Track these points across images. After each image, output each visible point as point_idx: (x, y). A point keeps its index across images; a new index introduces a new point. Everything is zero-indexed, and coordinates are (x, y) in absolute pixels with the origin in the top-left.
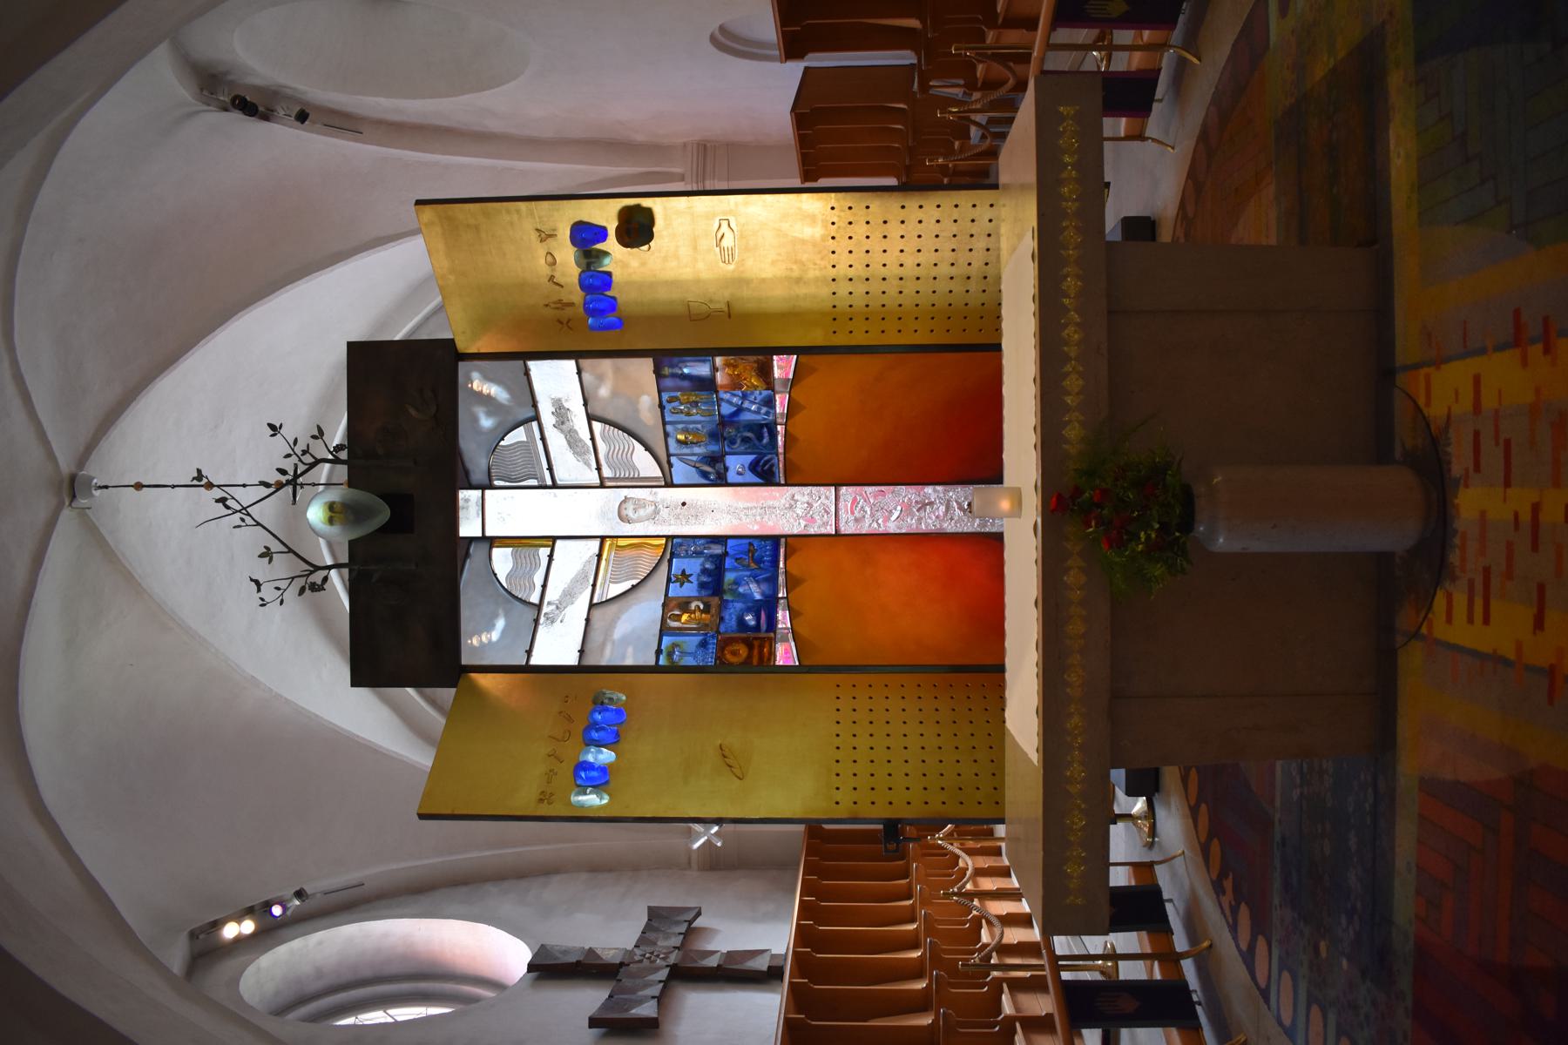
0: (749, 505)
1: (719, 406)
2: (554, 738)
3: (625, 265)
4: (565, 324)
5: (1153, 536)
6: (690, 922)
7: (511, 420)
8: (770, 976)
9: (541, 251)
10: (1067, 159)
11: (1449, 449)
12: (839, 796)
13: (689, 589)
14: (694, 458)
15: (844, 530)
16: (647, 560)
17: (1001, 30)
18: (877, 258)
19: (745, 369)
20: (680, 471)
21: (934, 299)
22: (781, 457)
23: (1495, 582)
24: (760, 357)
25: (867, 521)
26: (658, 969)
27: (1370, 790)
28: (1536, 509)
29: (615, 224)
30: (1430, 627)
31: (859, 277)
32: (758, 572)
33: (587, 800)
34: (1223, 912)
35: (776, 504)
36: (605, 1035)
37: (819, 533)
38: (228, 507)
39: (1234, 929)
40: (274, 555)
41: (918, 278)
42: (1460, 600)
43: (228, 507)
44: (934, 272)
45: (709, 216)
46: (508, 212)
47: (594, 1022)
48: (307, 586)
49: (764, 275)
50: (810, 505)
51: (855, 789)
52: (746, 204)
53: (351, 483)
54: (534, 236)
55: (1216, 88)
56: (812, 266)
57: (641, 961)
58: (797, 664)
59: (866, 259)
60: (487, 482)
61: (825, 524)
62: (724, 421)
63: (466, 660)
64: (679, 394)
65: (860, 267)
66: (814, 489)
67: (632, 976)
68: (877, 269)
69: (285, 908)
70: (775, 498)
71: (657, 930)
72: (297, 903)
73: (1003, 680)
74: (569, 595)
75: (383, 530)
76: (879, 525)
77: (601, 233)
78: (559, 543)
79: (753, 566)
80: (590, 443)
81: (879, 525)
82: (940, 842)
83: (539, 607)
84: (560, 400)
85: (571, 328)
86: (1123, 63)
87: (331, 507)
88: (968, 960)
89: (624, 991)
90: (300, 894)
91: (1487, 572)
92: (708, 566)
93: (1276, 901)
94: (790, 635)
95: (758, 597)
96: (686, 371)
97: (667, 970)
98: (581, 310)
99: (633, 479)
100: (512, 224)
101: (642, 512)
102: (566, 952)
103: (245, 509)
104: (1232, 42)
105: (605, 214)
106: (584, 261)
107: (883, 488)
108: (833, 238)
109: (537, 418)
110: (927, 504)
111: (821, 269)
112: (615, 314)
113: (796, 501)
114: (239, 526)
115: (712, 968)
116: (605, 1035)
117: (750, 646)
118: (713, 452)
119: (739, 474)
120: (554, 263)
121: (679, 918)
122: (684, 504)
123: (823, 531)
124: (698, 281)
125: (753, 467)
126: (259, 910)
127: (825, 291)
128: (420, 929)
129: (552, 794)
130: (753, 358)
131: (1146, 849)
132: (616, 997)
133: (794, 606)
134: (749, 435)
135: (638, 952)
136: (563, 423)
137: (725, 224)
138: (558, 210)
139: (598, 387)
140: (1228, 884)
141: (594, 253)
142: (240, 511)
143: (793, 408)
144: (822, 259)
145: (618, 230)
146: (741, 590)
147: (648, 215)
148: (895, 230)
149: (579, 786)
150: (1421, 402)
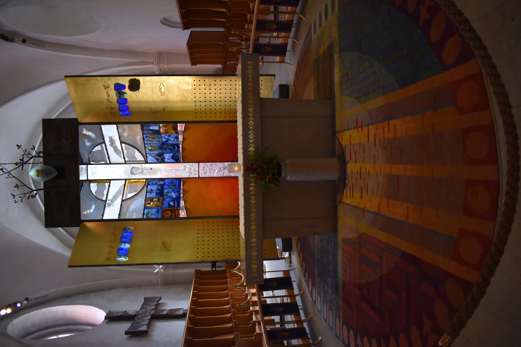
0: (171, 169)
1: (161, 139)
2: (111, 241)
3: (131, 96)
4: (113, 114)
5: (270, 177)
6: (158, 301)
7: (96, 143)
8: (182, 316)
9: (104, 92)
10: (250, 76)
11: (346, 154)
12: (198, 255)
13: (153, 195)
14: (154, 155)
15: (201, 176)
16: (140, 186)
17: (249, 24)
18: (208, 95)
19: (169, 127)
20: (150, 158)
21: (226, 107)
22: (181, 154)
23: (354, 187)
24: (174, 124)
25: (208, 173)
26: (147, 316)
27: (333, 243)
28: (361, 168)
29: (128, 84)
30: (343, 200)
31: (203, 101)
32: (175, 189)
33: (122, 259)
34: (306, 283)
35: (180, 168)
36: (130, 337)
37: (193, 177)
38: (3, 172)
39: (308, 286)
40: (19, 187)
41: (220, 101)
42: (348, 192)
43: (3, 172)
44: (225, 99)
45: (157, 82)
46: (94, 80)
47: (127, 333)
48: (30, 196)
49: (174, 100)
50: (190, 169)
51: (203, 253)
52: (168, 79)
53: (45, 163)
54: (103, 87)
55: (301, 50)
56: (188, 97)
57: (142, 314)
58: (186, 216)
59: (205, 95)
60: (88, 162)
61: (195, 174)
62: (163, 143)
63: (82, 218)
64: (149, 135)
65: (203, 98)
66: (192, 164)
67: (139, 318)
68: (208, 98)
69: (22, 304)
70: (179, 167)
71: (147, 304)
72: (26, 302)
73: (239, 219)
74: (115, 198)
75: (56, 178)
76: (211, 174)
77: (124, 87)
78: (112, 181)
79: (173, 187)
80: (121, 150)
81: (211, 174)
82: (235, 271)
83: (106, 201)
84: (111, 137)
85: (114, 115)
86: (280, 41)
87: (38, 171)
88: (240, 304)
89: (137, 323)
90: (27, 299)
91: (353, 184)
92: (159, 188)
93: (316, 276)
94: (184, 208)
95: (174, 197)
96: (151, 128)
97: (150, 316)
98: (118, 110)
99: (135, 161)
100: (95, 83)
101: (138, 171)
102: (117, 313)
103: (9, 172)
104: (304, 38)
105: (125, 81)
106: (118, 95)
107: (213, 163)
108: (195, 89)
109: (104, 142)
110: (226, 168)
111: (191, 98)
112: (129, 111)
113: (186, 167)
114: (7, 178)
115: (165, 315)
116: (130, 337)
117: (172, 212)
118: (160, 153)
119: (168, 159)
120: (109, 95)
121: (154, 301)
122: (151, 169)
123: (195, 176)
124: (154, 102)
125: (173, 157)
126: (13, 305)
127: (193, 105)
128: (68, 309)
129: (110, 258)
130: (171, 124)
131: (289, 267)
132: (134, 325)
133: (185, 199)
134: (171, 147)
135: (141, 311)
136: (112, 144)
137: (162, 85)
138: (110, 80)
139: (124, 133)
140: (307, 274)
141: (121, 93)
142: (7, 173)
143: (184, 139)
144: (192, 95)
145: (129, 86)
146: (169, 195)
147: (138, 81)
148: (213, 88)
149: (119, 255)
150: (341, 141)
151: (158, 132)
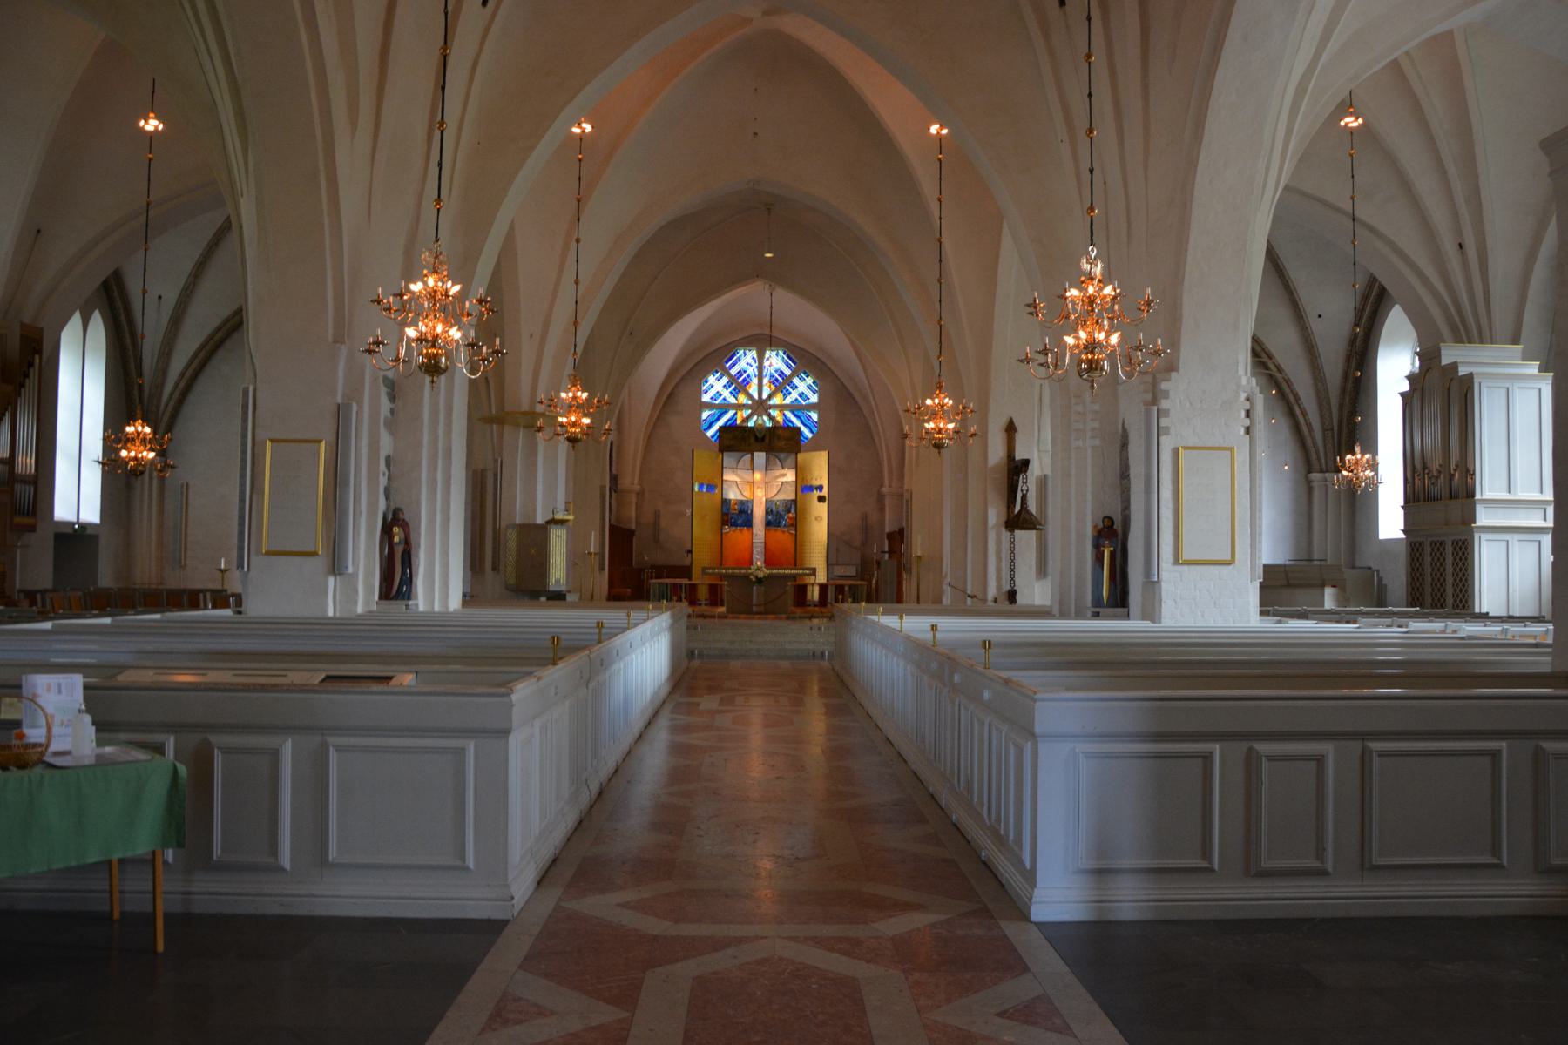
63: (725, 453)
75: (756, 436)
77: (821, 491)
147: (824, 502)
151: (789, 512)
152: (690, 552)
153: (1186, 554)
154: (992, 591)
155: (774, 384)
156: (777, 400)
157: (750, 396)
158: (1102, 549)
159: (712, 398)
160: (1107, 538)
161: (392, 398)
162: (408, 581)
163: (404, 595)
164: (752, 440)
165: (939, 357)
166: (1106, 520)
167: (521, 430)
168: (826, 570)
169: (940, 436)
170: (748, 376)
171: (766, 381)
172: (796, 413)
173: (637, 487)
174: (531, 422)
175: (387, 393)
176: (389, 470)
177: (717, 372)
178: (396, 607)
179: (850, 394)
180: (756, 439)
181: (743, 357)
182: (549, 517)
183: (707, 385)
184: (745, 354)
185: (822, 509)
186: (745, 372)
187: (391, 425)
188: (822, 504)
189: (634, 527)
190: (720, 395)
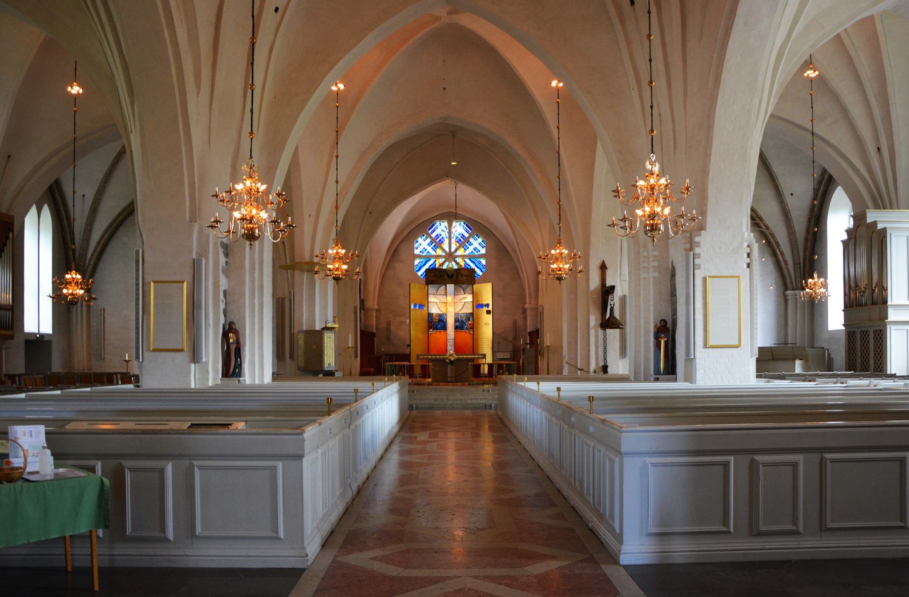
77: (488, 307)
127: (480, 337)
151: (469, 320)
152: (409, 345)
153: (711, 342)
154: (593, 366)
155: (458, 242)
156: (461, 252)
157: (444, 250)
158: (660, 339)
159: (421, 252)
160: (663, 333)
161: (227, 255)
162: (239, 366)
163: (237, 374)
164: (446, 277)
165: (559, 224)
166: (662, 322)
167: (305, 273)
168: (492, 354)
169: (560, 272)
170: (443, 238)
171: (453, 241)
172: (472, 260)
173: (376, 307)
174: (311, 268)
175: (224, 252)
176: (226, 299)
177: (423, 236)
178: (232, 382)
179: (505, 248)
180: (449, 276)
181: (439, 227)
182: (323, 326)
183: (417, 244)
184: (440, 225)
185: (489, 319)
186: (440, 235)
187: (225, 271)
188: (489, 315)
189: (375, 331)
190: (426, 250)
